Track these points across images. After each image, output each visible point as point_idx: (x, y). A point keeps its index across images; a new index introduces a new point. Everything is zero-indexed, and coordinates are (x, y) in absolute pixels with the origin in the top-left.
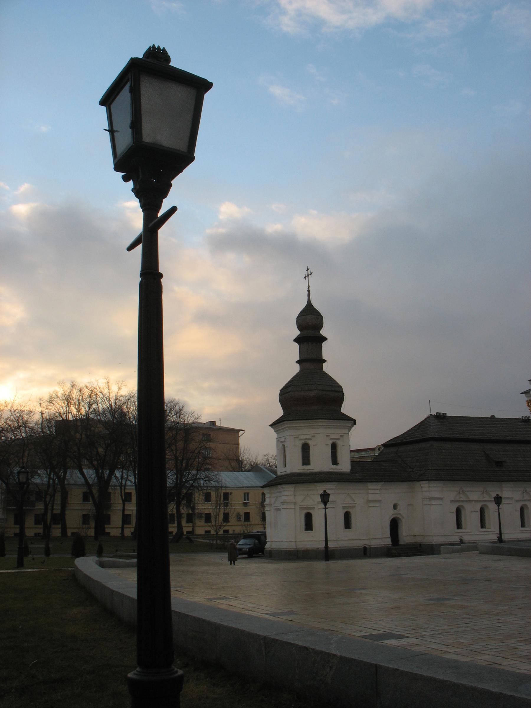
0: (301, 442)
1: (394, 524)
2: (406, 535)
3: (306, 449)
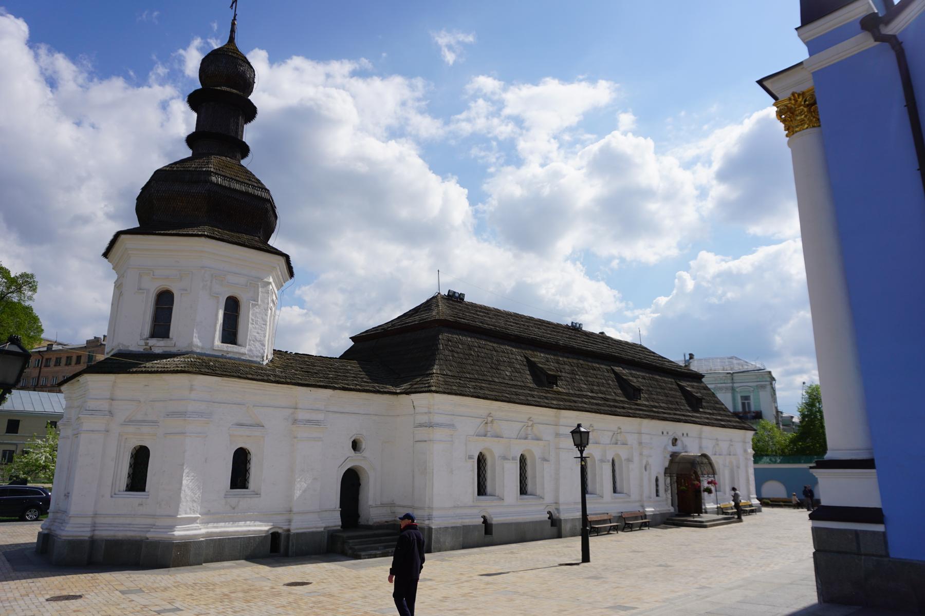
0: (153, 287)
1: (351, 482)
2: (375, 504)
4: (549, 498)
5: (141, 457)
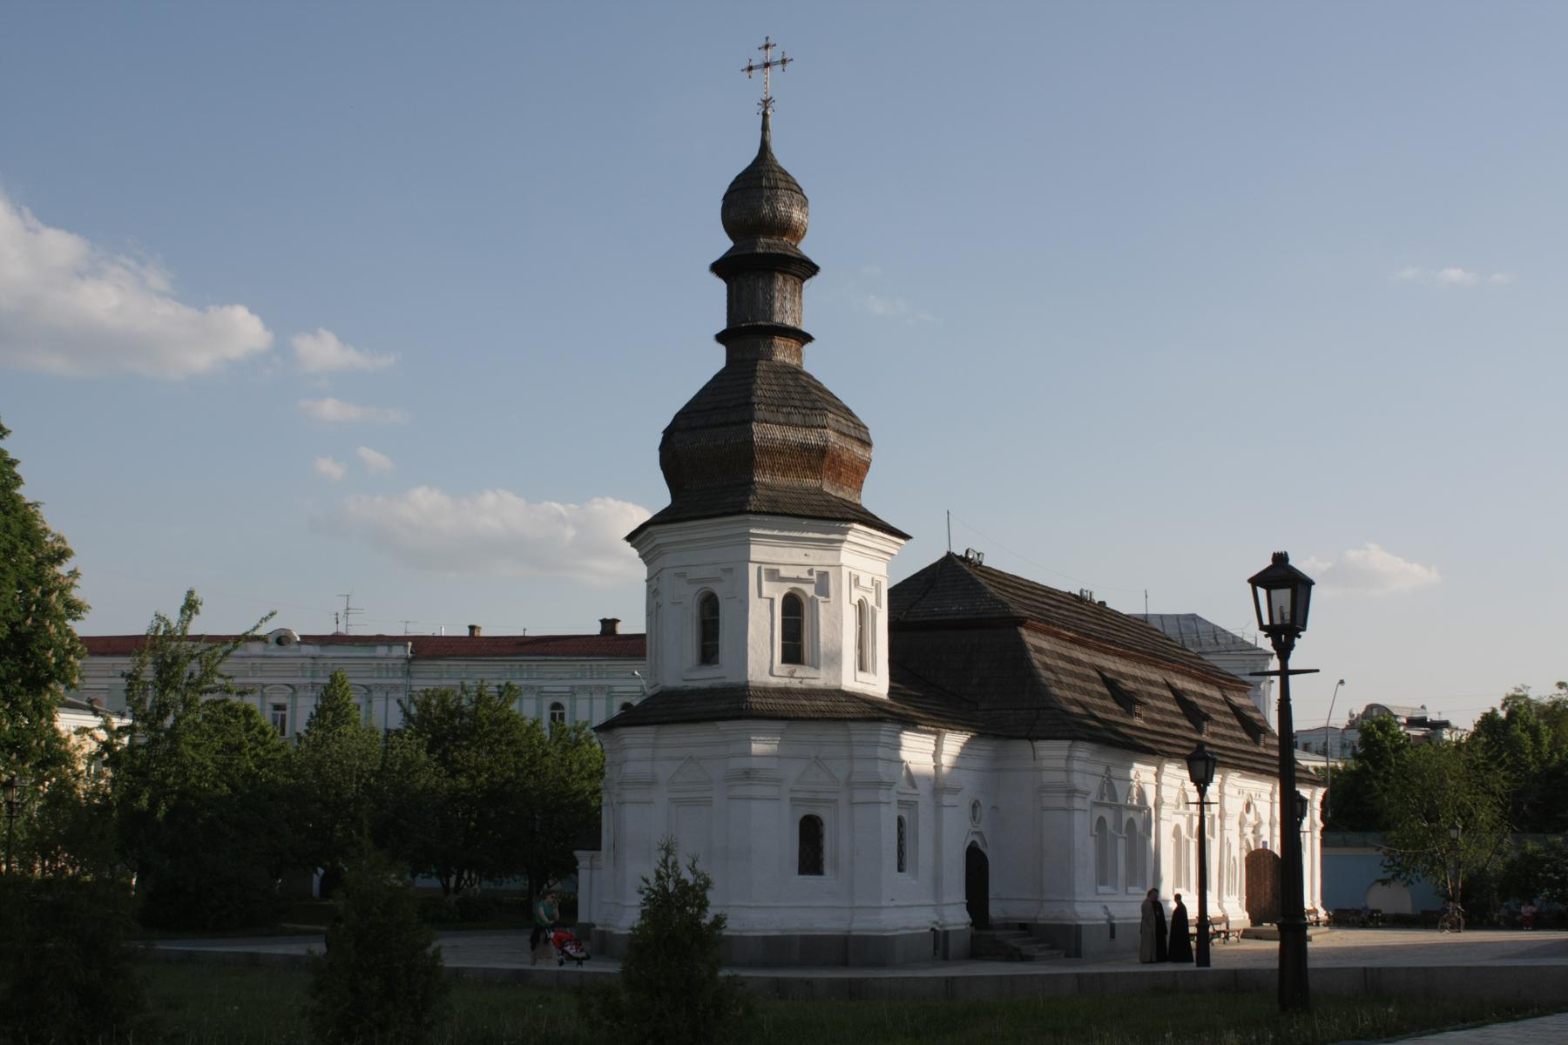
3: (794, 610)
4: (1150, 887)
5: (811, 832)
